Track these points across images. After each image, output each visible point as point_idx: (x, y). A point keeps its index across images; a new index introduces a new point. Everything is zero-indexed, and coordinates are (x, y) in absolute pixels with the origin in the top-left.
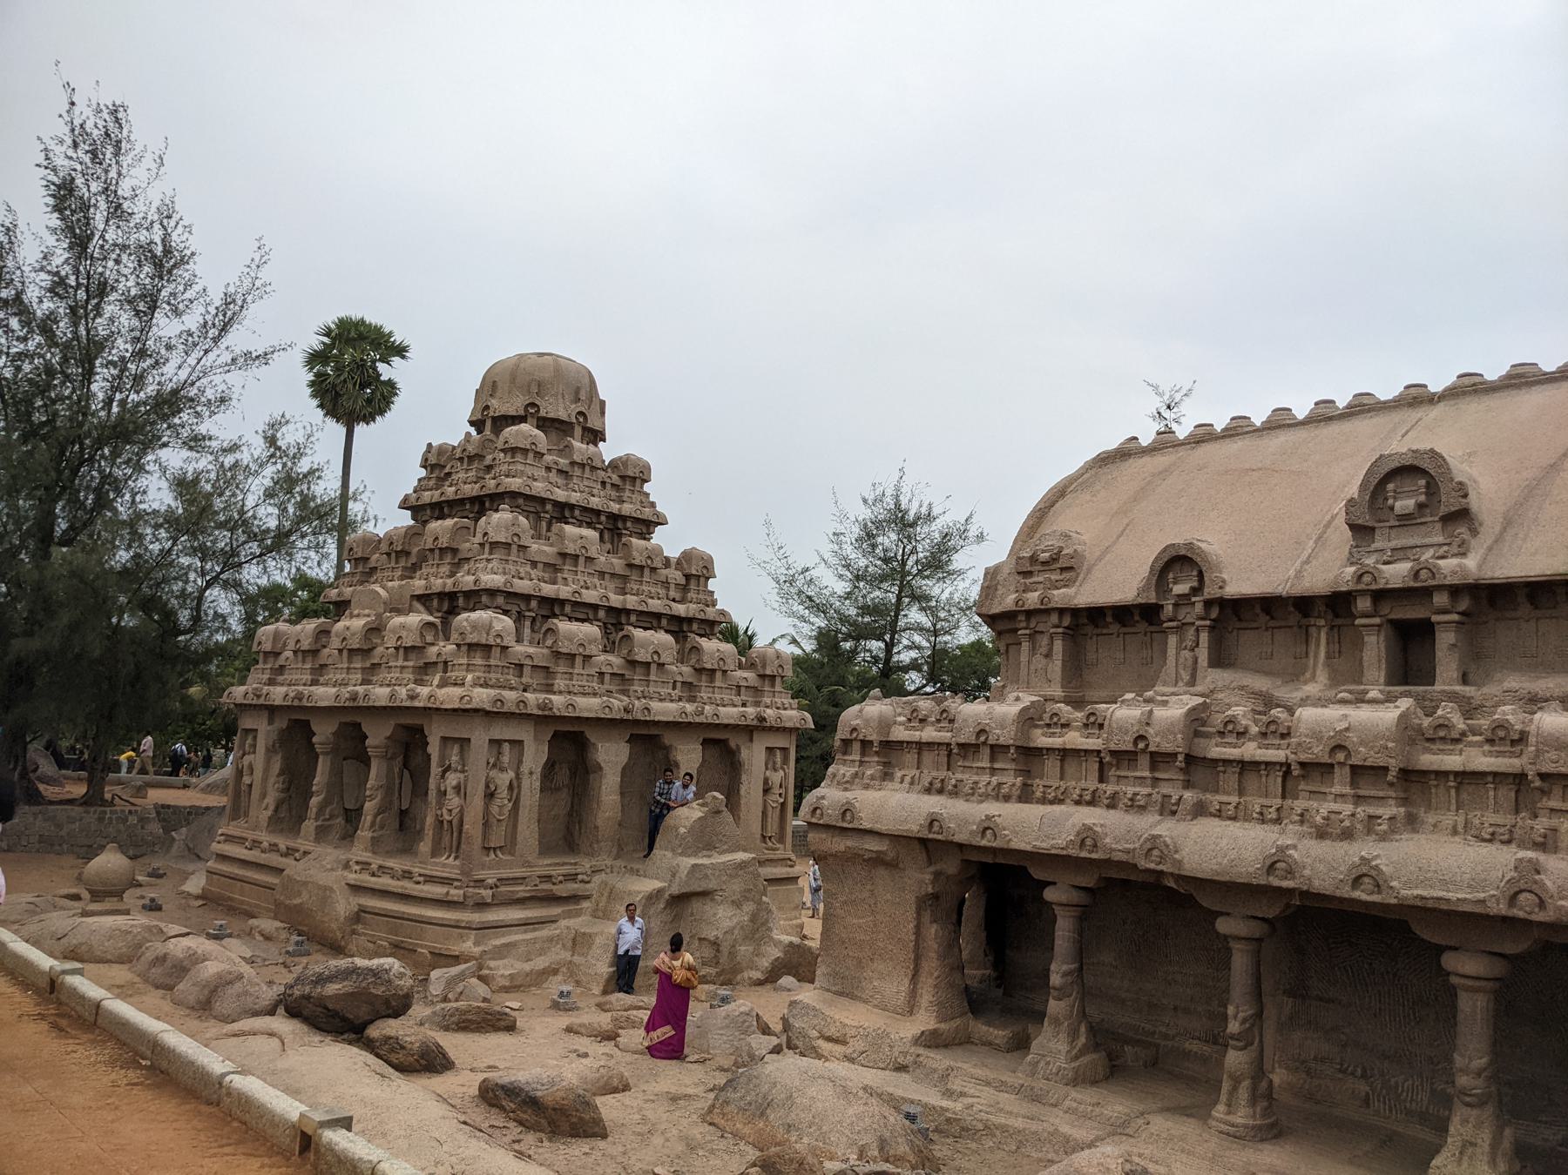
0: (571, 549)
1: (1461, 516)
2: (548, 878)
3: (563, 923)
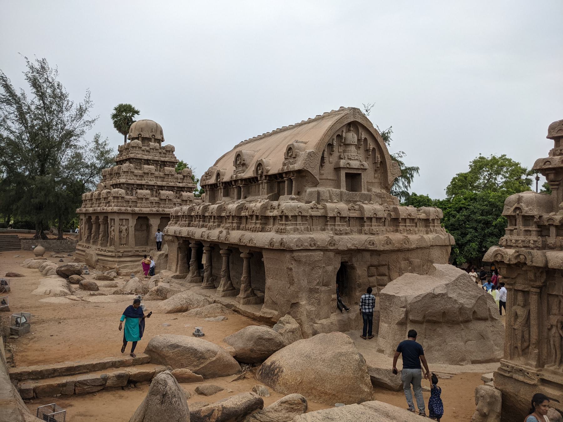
0: (146, 171)
1: (244, 165)
2: (138, 251)
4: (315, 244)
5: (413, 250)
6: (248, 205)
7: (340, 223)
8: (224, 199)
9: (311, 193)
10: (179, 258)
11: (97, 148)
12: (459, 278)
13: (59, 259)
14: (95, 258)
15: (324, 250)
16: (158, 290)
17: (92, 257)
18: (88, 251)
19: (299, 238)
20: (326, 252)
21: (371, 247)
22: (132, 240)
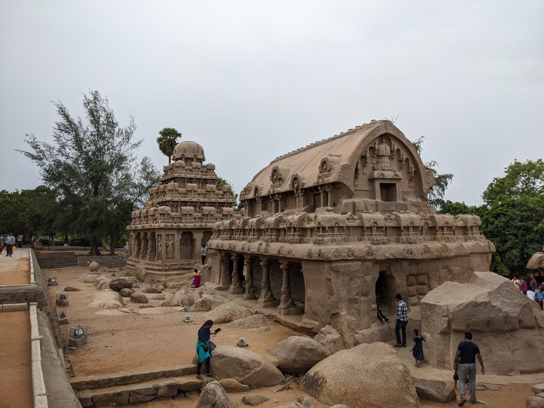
1: (280, 179)
3: (187, 274)
4: (352, 255)
5: (452, 258)
6: (285, 218)
7: (376, 233)
8: (262, 212)
9: (347, 205)
10: (222, 270)
11: (144, 169)
12: (501, 285)
13: (112, 274)
14: (144, 272)
15: (362, 260)
16: (203, 302)
17: (141, 272)
18: (137, 265)
19: (337, 249)
20: (364, 263)
21: (410, 257)
22: (177, 254)
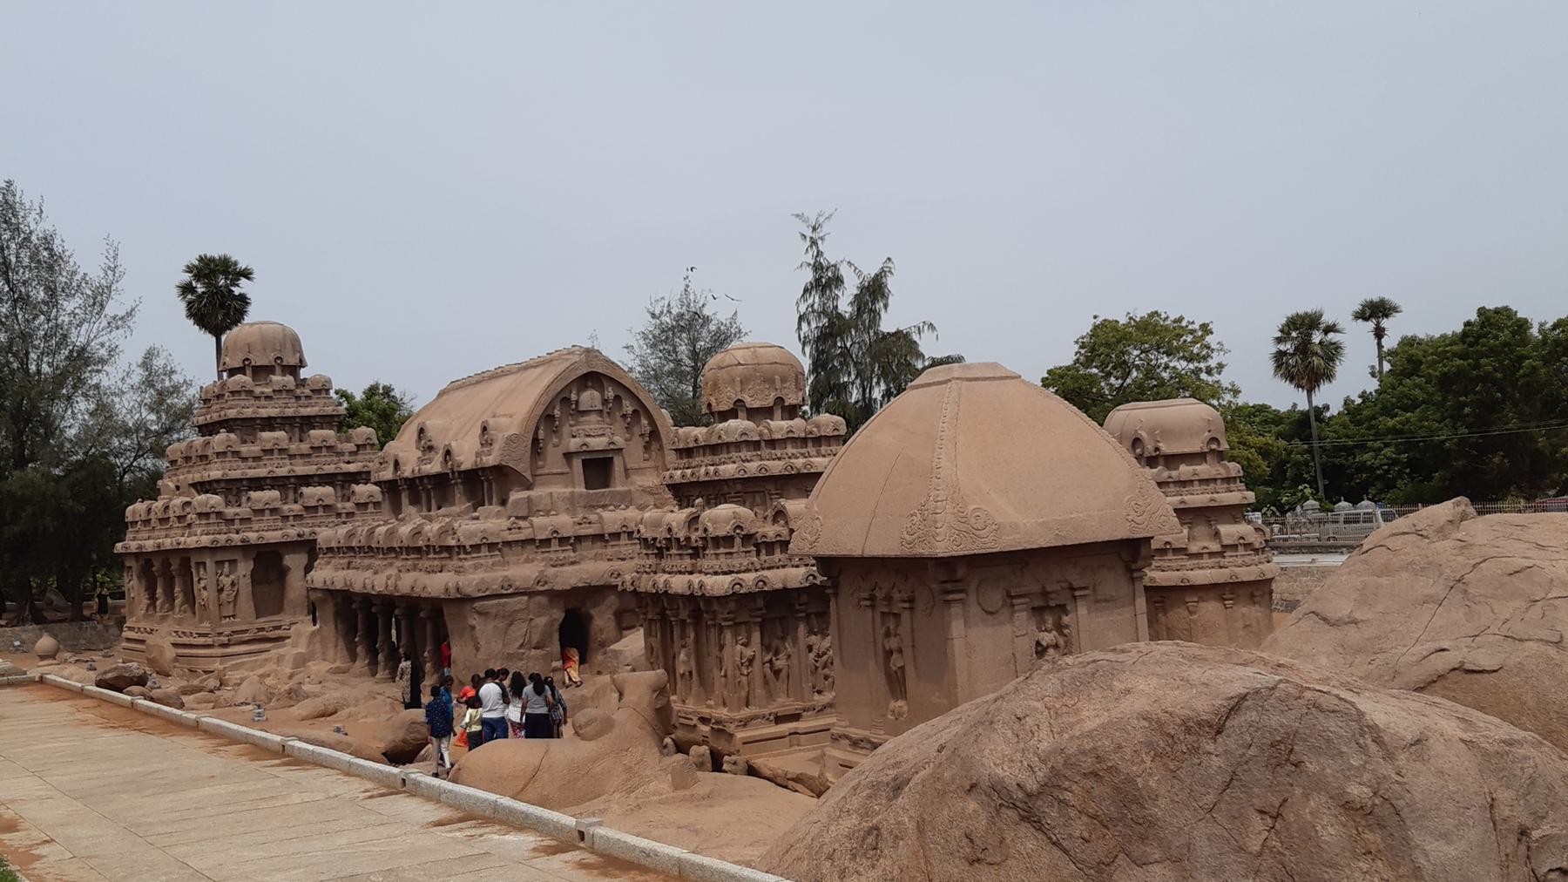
9: (517, 502)
11: (149, 383)
15: (531, 594)
